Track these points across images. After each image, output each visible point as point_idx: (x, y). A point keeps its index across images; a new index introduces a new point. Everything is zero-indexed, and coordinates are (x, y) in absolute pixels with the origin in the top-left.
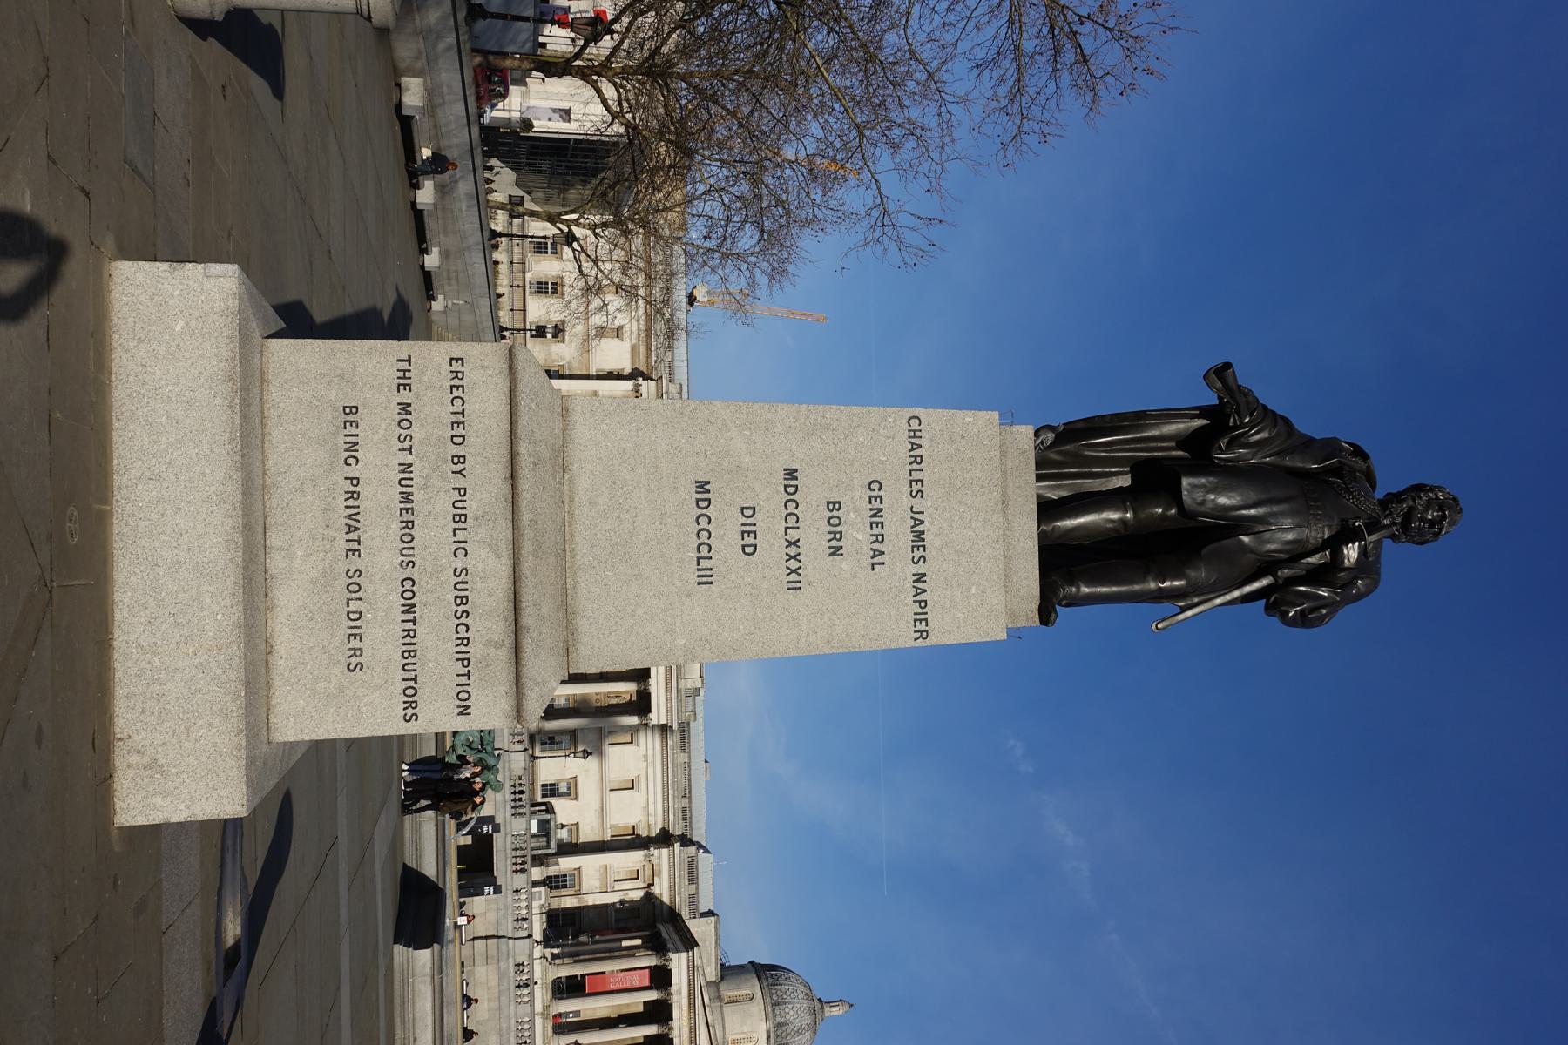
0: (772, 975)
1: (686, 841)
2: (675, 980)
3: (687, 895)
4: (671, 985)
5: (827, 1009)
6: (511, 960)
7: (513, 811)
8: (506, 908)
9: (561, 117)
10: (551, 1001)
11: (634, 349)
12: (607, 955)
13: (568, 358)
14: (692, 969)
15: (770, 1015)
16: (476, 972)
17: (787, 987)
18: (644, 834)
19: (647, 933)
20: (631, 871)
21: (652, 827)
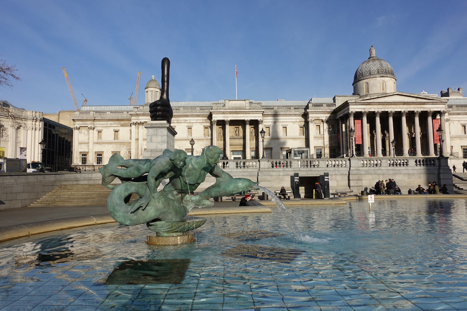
0: (359, 76)
1: (307, 107)
2: (360, 110)
3: (327, 107)
4: (361, 112)
5: (373, 56)
7: (289, 167)
8: (335, 171)
9: (24, 151)
11: (122, 126)
13: (126, 150)
14: (356, 103)
15: (374, 76)
16: (365, 185)
17: (364, 70)
18: (303, 123)
19: (340, 122)
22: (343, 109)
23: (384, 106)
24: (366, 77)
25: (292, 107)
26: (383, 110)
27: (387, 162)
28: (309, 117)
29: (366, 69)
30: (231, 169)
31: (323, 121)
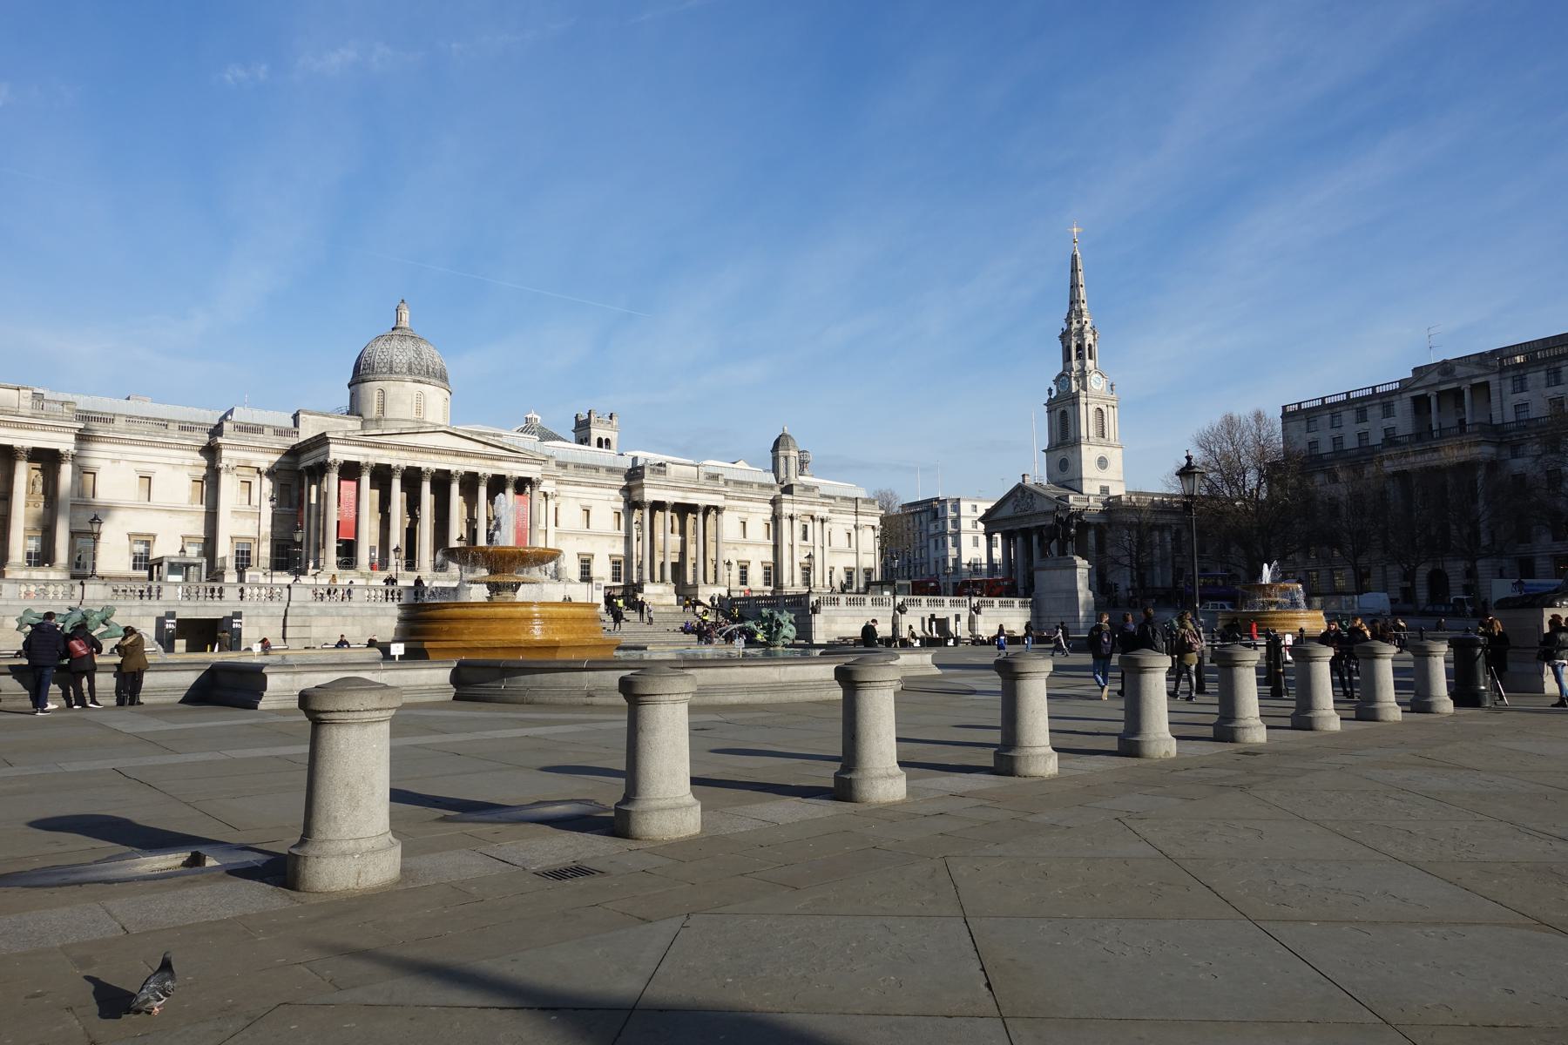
1: (217, 431)
4: (359, 462)
5: (402, 324)
6: (309, 605)
8: (258, 607)
10: (357, 571)
12: (322, 518)
14: (346, 441)
16: (317, 636)
18: (204, 471)
19: (306, 479)
20: (241, 488)
21: (196, 463)
22: (316, 448)
23: (413, 455)
24: (381, 376)
25: (171, 424)
26: (410, 464)
27: (363, 594)
28: (221, 458)
29: (383, 357)
30: (7, 600)
31: (259, 471)
